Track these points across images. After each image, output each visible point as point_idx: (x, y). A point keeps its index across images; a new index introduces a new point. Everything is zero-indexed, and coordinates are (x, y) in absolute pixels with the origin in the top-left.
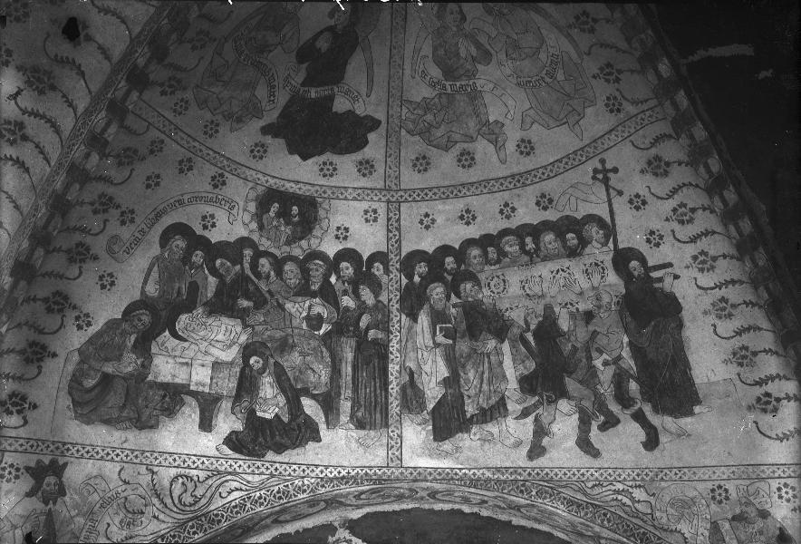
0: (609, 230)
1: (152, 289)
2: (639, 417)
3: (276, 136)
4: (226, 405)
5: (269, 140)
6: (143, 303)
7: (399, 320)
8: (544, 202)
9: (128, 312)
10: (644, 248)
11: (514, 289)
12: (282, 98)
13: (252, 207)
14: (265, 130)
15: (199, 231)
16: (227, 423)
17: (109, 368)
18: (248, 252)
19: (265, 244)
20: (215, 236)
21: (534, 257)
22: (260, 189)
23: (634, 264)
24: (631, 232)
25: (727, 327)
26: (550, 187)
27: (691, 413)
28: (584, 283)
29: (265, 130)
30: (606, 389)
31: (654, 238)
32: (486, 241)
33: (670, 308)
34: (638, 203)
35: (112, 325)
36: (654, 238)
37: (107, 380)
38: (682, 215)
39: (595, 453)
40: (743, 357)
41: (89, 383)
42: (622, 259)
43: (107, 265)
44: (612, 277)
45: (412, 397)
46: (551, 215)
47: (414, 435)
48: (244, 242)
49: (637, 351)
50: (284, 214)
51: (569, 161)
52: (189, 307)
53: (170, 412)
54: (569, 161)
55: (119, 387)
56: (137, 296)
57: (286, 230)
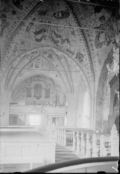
1: (96, 35)
3: (96, 13)
4: (105, 42)
5: (96, 14)
6: (97, 36)
7: (113, 23)
9: (96, 37)
12: (93, 9)
13: (99, 21)
14: (95, 13)
15: (97, 26)
16: (106, 43)
17: (97, 43)
18: (102, 25)
19: (103, 23)
20: (98, 26)
22: (99, 19)
29: (95, 13)
35: (95, 40)
37: (97, 44)
41: (96, 45)
43: (92, 35)
48: (101, 24)
50: (102, 19)
52: (99, 35)
53: (102, 44)
55: (98, 45)
56: (96, 36)
57: (103, 20)
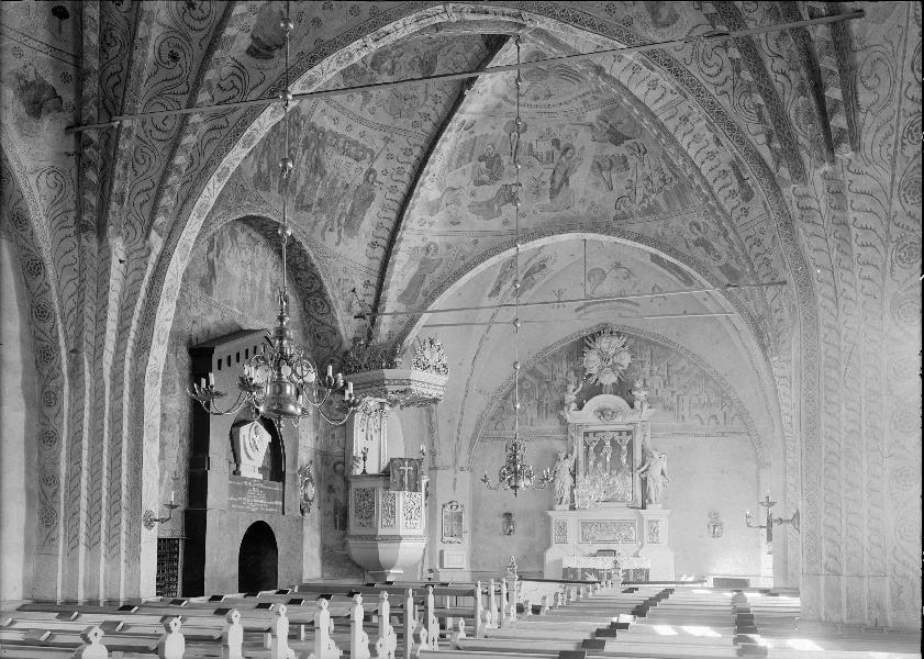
0: (373, 159)
2: (339, 232)
8: (362, 135)
10: (379, 172)
11: (331, 162)
21: (345, 152)
23: (372, 176)
24: (378, 166)
25: (383, 214)
26: (369, 131)
27: (350, 236)
28: (352, 172)
30: (336, 217)
31: (385, 172)
32: (336, 136)
33: (371, 198)
34: (390, 157)
36: (385, 172)
38: (400, 171)
39: (324, 239)
40: (379, 226)
42: (371, 171)
44: (362, 177)
45: (293, 190)
46: (361, 141)
47: (290, 206)
49: (353, 206)
51: (382, 128)
54: (382, 128)
